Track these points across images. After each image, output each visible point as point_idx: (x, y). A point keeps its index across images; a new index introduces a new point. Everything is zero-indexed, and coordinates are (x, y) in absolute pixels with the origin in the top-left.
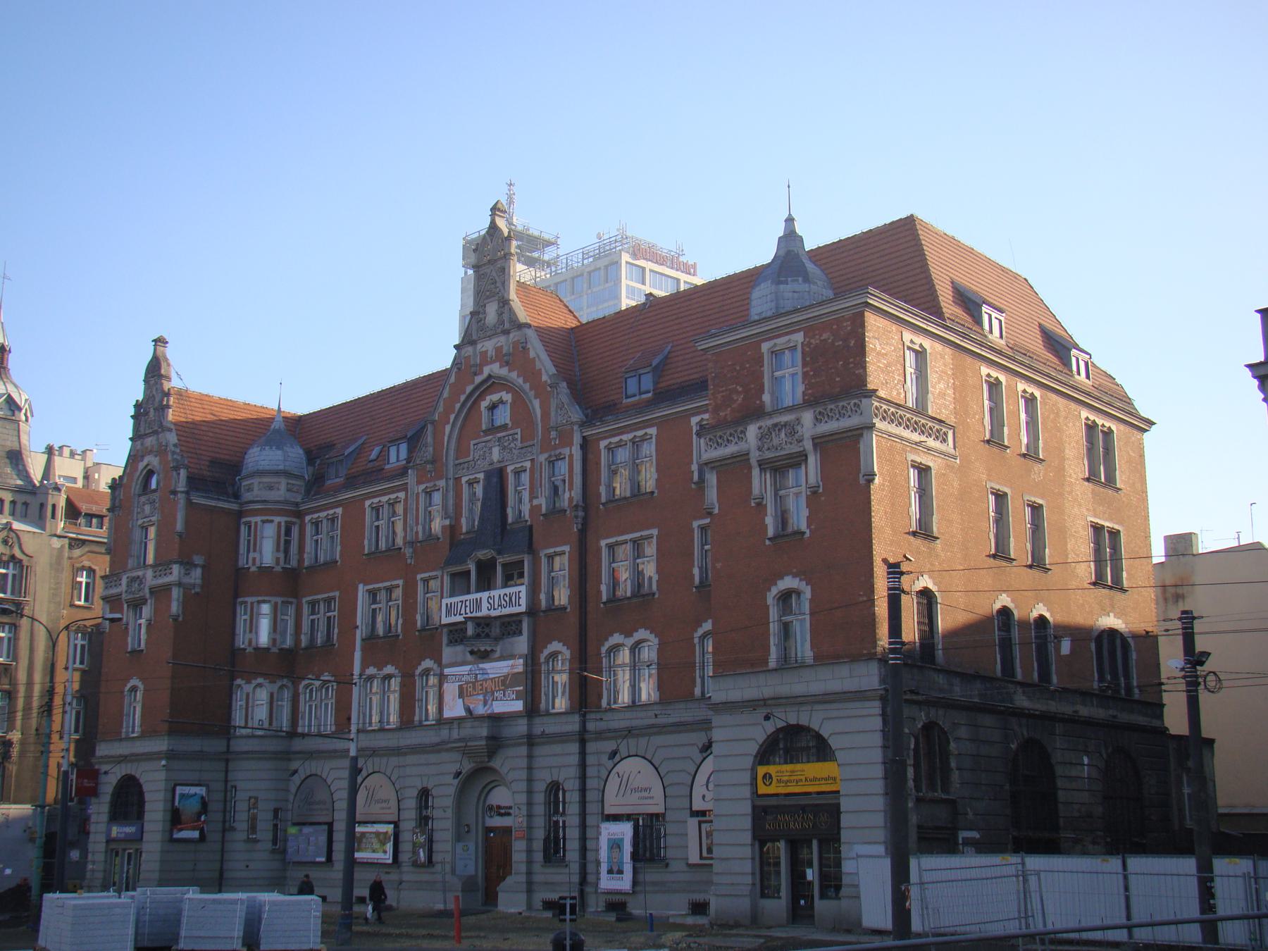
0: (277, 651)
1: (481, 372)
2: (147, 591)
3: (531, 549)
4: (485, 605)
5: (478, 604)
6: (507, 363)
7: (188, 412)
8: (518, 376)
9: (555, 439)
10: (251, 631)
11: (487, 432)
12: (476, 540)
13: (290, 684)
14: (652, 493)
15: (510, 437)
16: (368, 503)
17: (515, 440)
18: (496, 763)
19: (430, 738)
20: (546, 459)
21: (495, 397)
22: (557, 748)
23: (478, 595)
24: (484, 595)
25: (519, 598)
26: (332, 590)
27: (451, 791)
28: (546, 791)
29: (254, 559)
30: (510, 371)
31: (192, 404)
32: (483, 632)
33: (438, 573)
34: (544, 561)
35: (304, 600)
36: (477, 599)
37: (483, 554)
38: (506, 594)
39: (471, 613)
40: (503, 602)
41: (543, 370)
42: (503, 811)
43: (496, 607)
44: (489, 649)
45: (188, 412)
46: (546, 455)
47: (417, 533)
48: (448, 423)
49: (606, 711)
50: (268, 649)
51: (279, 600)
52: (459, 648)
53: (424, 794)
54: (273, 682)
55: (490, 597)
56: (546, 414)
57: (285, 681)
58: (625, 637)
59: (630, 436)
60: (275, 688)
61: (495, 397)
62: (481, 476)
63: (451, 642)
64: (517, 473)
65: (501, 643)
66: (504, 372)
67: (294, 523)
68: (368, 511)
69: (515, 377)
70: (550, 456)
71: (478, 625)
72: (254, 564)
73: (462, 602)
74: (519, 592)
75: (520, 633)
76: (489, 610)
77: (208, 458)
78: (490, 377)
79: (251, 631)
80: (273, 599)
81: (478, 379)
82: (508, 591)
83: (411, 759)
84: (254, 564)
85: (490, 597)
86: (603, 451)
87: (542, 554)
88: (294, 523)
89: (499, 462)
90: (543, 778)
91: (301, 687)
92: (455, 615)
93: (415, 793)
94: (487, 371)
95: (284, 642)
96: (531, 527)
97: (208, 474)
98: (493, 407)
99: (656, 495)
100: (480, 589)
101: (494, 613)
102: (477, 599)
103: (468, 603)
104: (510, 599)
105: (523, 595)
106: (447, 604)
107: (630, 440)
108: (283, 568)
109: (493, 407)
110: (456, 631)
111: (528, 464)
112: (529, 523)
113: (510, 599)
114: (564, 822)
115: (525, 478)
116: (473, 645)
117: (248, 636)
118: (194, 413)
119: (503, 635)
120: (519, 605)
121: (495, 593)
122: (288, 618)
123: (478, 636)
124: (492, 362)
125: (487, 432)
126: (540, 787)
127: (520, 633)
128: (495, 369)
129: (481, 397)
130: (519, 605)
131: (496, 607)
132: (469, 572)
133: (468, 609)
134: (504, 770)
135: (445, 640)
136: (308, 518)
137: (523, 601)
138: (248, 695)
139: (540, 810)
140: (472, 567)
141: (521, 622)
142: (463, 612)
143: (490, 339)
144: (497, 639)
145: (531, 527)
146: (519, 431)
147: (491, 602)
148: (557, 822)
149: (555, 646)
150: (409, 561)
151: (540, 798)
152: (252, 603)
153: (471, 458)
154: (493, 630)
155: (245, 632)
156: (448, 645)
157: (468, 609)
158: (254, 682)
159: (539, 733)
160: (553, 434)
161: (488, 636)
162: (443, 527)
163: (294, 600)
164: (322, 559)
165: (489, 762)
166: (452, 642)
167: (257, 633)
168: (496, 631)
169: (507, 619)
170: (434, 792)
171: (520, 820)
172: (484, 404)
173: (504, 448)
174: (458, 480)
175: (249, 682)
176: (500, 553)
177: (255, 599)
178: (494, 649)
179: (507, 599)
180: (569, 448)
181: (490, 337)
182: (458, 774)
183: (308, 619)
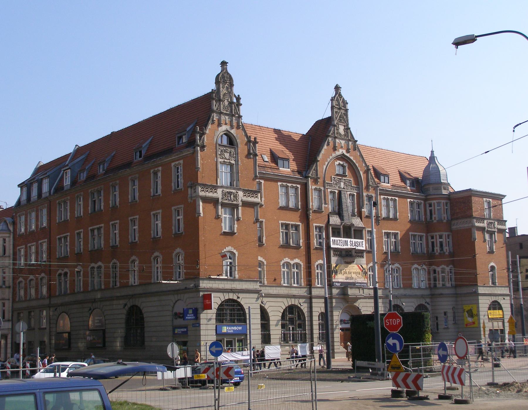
4: (349, 243)
16: (173, 164)
23: (346, 239)
24: (349, 240)
25: (363, 244)
39: (344, 246)
40: (356, 244)
43: (353, 245)
61: (341, 163)
69: (335, 154)
74: (362, 242)
75: (363, 257)
82: (356, 240)
92: (344, 246)
106: (333, 240)
117: (321, 241)
122: (291, 231)
127: (363, 257)
131: (353, 245)
133: (342, 243)
142: (340, 244)
147: (352, 243)
157: (342, 243)
179: (358, 243)
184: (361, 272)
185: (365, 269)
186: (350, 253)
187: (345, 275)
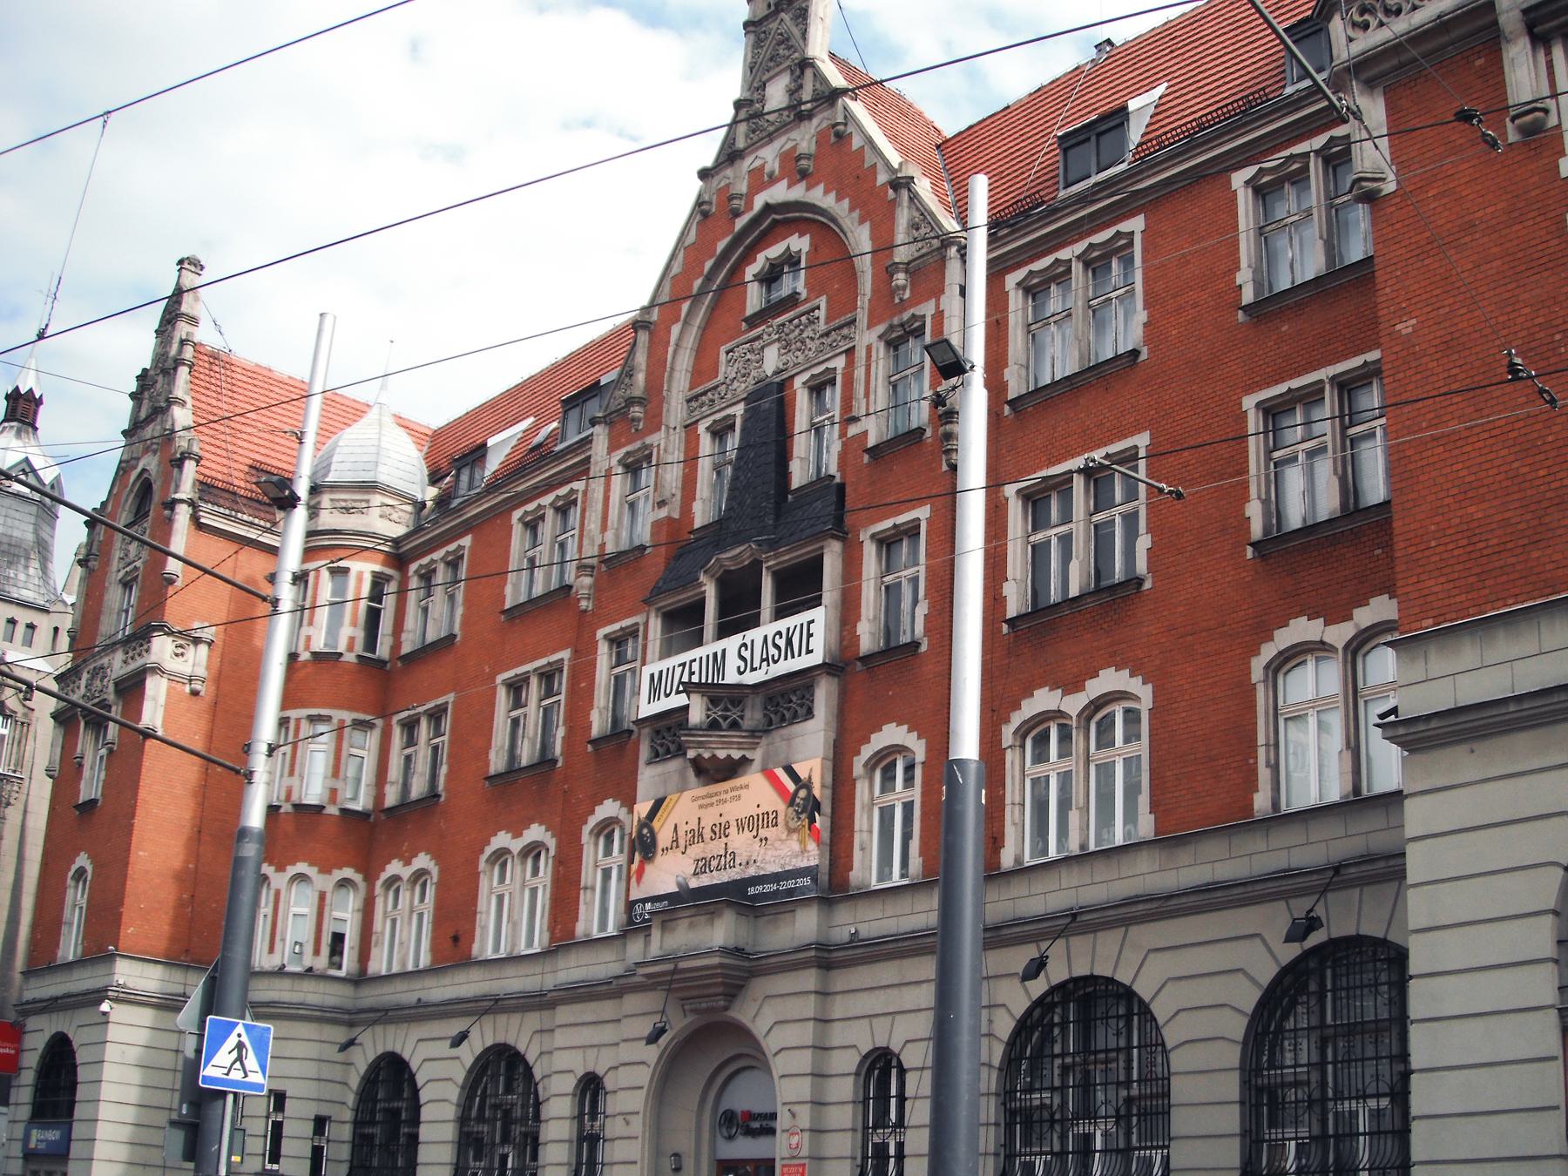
0: (337, 813)
1: (749, 205)
2: (111, 688)
3: (841, 529)
4: (733, 662)
5: (719, 661)
6: (804, 175)
7: (224, 385)
8: (826, 192)
9: (904, 288)
10: (291, 773)
11: (754, 320)
12: (719, 533)
13: (358, 878)
14: (1135, 353)
15: (803, 319)
17: (811, 322)
18: (742, 1013)
19: (601, 966)
20: (880, 337)
21: (775, 251)
22: (887, 972)
23: (718, 646)
24: (732, 643)
25: (810, 635)
26: (444, 693)
27: (643, 1076)
28: (857, 1074)
29: (309, 638)
30: (808, 188)
31: (234, 375)
32: (725, 718)
33: (639, 619)
34: (870, 551)
35: (395, 719)
36: (715, 655)
37: (734, 556)
38: (779, 633)
40: (773, 651)
41: (880, 166)
42: (756, 1125)
44: (736, 755)
45: (223, 378)
46: (881, 329)
47: (603, 546)
48: (677, 320)
49: (1021, 871)
50: (319, 809)
51: (348, 716)
52: (674, 765)
53: (591, 1087)
54: (326, 870)
55: (745, 645)
56: (883, 247)
57: (348, 872)
58: (1066, 693)
59: (1079, 247)
60: (325, 882)
61: (775, 251)
62: (739, 410)
63: (657, 755)
64: (818, 389)
65: (764, 741)
66: (798, 193)
67: (388, 579)
68: (517, 529)
70: (891, 328)
71: (714, 701)
72: (307, 647)
73: (684, 665)
76: (741, 673)
77: (250, 462)
78: (768, 208)
79: (291, 773)
80: (340, 715)
81: (740, 223)
82: (784, 624)
83: (564, 1014)
84: (307, 647)
85: (745, 645)
86: (1012, 295)
87: (864, 536)
88: (388, 579)
89: (778, 372)
90: (859, 1039)
91: (379, 883)
93: (568, 1084)
94: (759, 202)
95: (355, 798)
96: (841, 488)
97: (242, 484)
98: (770, 278)
99: (1144, 356)
100: (724, 631)
101: (750, 678)
102: (715, 655)
103: (695, 667)
104: (789, 642)
105: (818, 630)
106: (652, 676)
107: (1078, 257)
108: (359, 657)
109: (770, 278)
110: (669, 729)
111: (839, 363)
112: (838, 480)
113: (789, 642)
114: (900, 1146)
115: (833, 397)
116: (701, 745)
118: (235, 389)
119: (770, 723)
120: (809, 652)
121: (755, 635)
123: (714, 725)
124: (773, 180)
125: (754, 320)
126: (846, 1062)
127: (810, 714)
128: (780, 193)
129: (747, 257)
130: (809, 652)
131: (756, 664)
132: (700, 605)
134: (759, 1028)
135: (644, 752)
136: (413, 567)
137: (818, 643)
138: (278, 893)
139: (843, 1117)
140: (710, 592)
141: (810, 689)
143: (771, 141)
144: (755, 734)
145: (841, 488)
146: (823, 302)
147: (747, 654)
148: (881, 1150)
149: (891, 734)
150: (584, 604)
151: (844, 1089)
152: (298, 720)
153: (721, 378)
154: (748, 714)
155: (282, 776)
156: (649, 763)
158: (292, 870)
159: (846, 937)
160: (900, 278)
161: (735, 725)
162: (656, 525)
163: (379, 722)
164: (431, 637)
165: (726, 1008)
166: (657, 757)
167: (301, 777)
168: (753, 716)
169: (780, 687)
170: (609, 1083)
171: (795, 1140)
172: (751, 271)
173: (787, 347)
174: (690, 428)
175: (281, 868)
176: (773, 545)
177: (304, 712)
178: (749, 755)
179: (782, 643)
180: (932, 302)
181: (770, 138)
182: (653, 1039)
183: (401, 754)
184: (781, 806)
185: (807, 785)
186: (717, 713)
187: (696, 851)
